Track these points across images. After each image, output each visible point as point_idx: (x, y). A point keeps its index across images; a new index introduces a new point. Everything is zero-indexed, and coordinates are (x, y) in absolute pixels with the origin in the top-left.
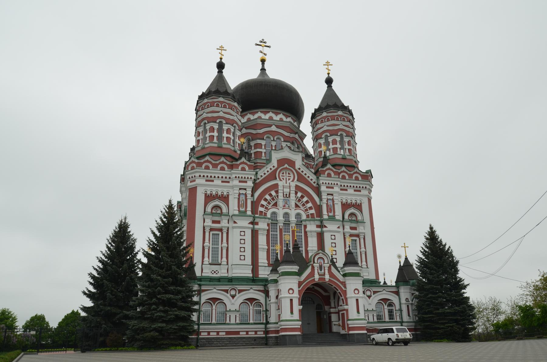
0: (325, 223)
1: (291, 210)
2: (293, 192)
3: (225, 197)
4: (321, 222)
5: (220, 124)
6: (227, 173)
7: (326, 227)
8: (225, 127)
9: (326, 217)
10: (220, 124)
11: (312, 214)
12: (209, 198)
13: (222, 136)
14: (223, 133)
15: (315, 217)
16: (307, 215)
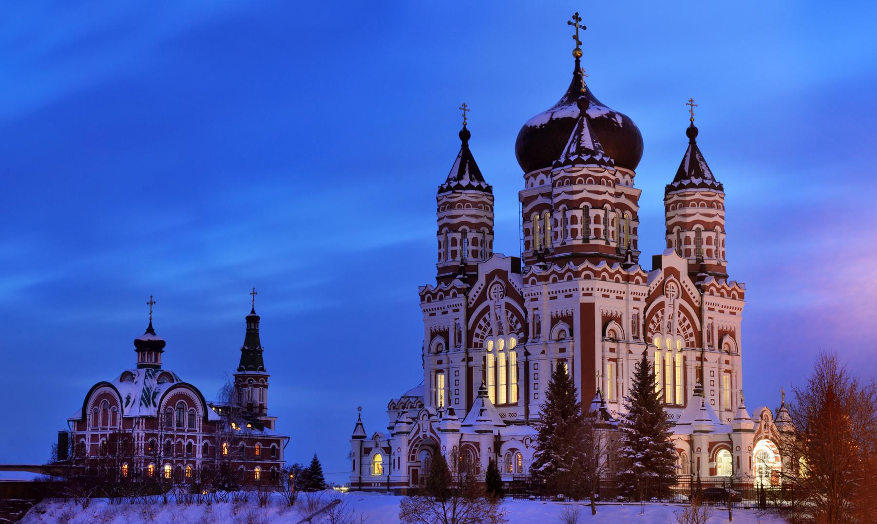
0: (707, 355)
1: (672, 335)
2: (676, 315)
3: (618, 318)
4: (703, 352)
5: (586, 210)
6: (621, 287)
7: (706, 360)
8: (593, 213)
9: (706, 348)
10: (586, 210)
11: (692, 343)
12: (607, 320)
13: (588, 228)
14: (590, 223)
15: (695, 346)
16: (687, 343)
